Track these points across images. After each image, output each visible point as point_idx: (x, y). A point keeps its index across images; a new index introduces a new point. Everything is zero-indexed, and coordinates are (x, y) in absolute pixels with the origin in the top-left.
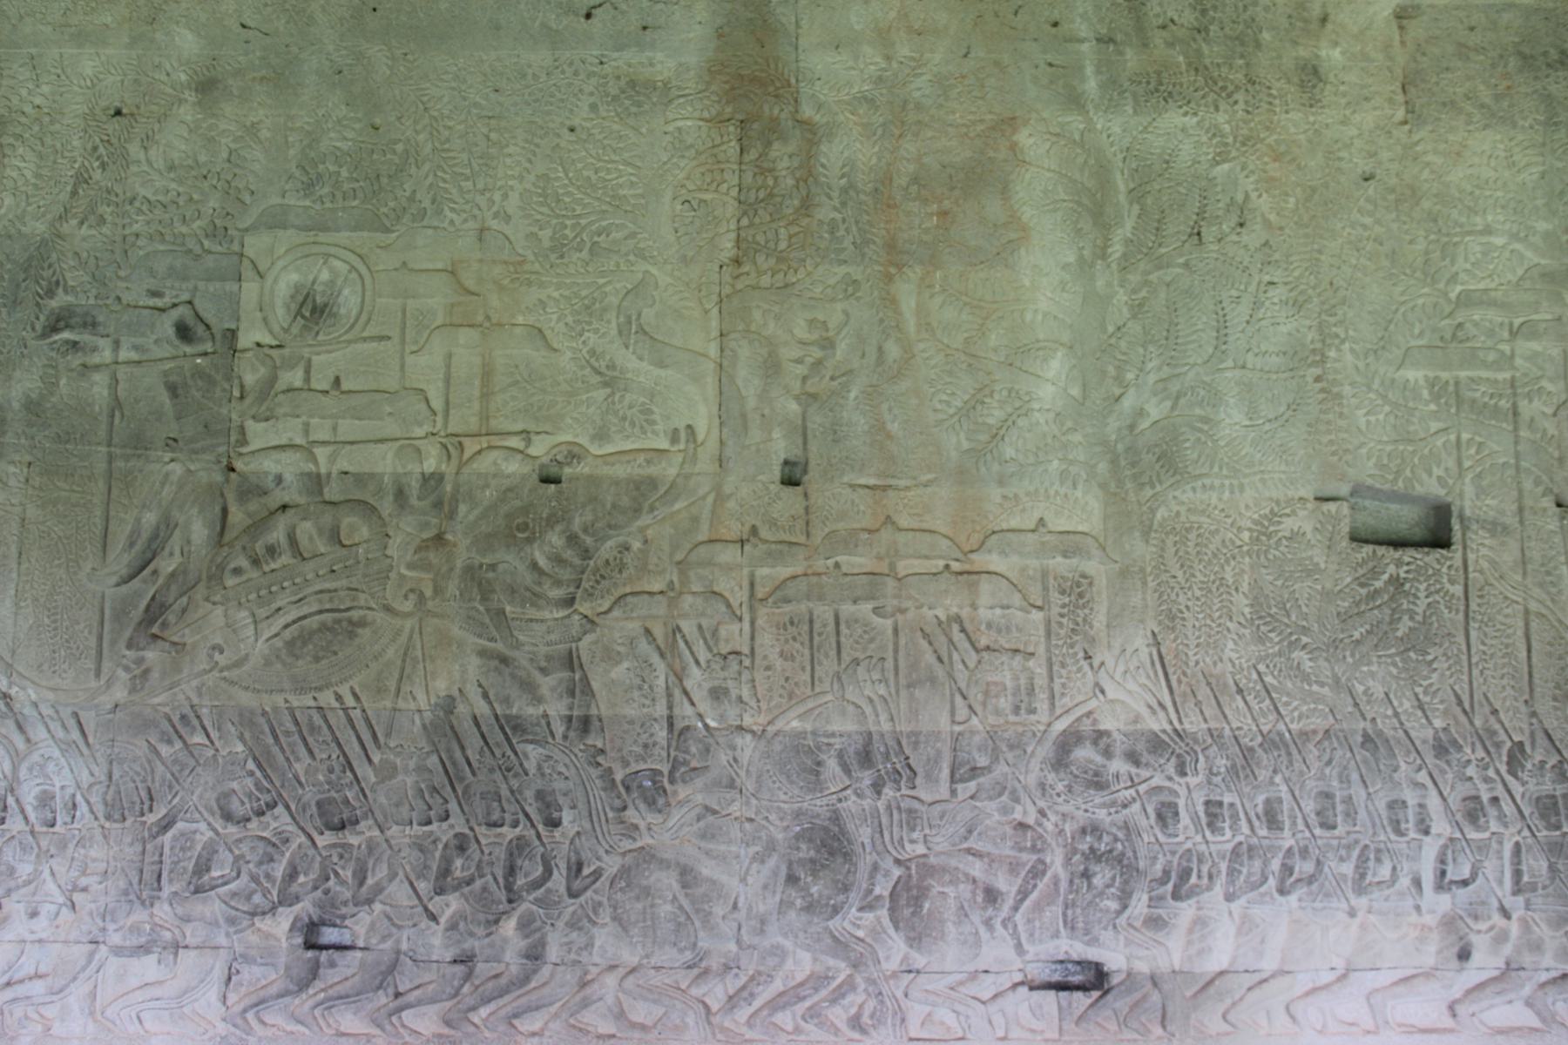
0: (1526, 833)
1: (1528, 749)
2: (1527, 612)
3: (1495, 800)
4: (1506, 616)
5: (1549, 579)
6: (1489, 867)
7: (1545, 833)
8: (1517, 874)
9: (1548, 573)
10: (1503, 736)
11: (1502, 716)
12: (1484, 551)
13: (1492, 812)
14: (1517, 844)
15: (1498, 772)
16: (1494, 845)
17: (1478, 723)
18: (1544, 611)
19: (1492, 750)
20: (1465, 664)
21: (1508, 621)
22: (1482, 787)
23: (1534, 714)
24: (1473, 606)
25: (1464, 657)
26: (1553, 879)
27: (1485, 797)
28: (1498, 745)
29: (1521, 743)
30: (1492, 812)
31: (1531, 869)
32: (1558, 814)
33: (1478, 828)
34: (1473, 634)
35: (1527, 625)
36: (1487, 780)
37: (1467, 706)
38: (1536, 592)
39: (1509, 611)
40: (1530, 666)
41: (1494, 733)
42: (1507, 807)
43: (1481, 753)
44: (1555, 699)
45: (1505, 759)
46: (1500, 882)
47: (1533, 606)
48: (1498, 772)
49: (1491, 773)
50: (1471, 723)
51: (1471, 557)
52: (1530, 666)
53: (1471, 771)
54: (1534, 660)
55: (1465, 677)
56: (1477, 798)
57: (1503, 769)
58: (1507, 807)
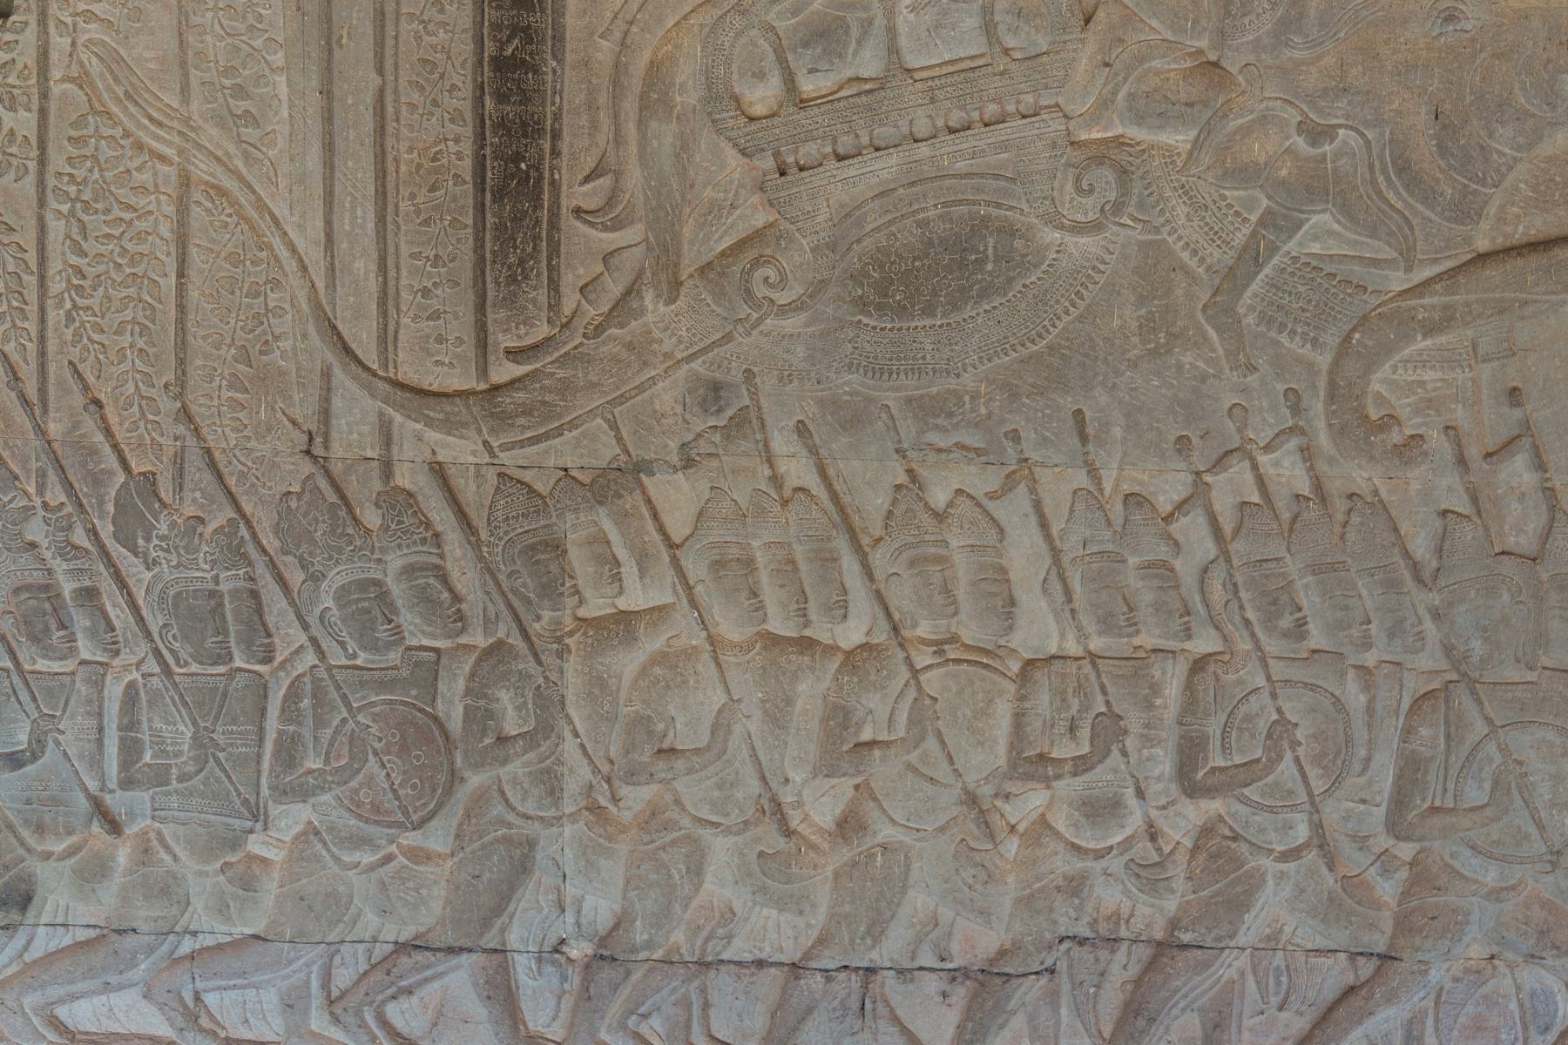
0: (152, 666)
1: (166, 491)
2: (185, 181)
3: (89, 595)
4: (142, 189)
5: (241, 106)
6: (72, 731)
7: (195, 668)
8: (131, 750)
9: (240, 92)
10: (112, 461)
11: (109, 411)
12: (93, 31)
13: (81, 621)
14: (131, 696)
15: (93, 532)
16: (82, 688)
17: (54, 429)
18: (228, 183)
19: (82, 488)
20: (32, 296)
21: (141, 202)
22: (60, 566)
23: (186, 415)
24: (57, 162)
25: (31, 280)
26: (201, 763)
27: (67, 588)
28: (98, 480)
29: (150, 479)
30: (81, 621)
31: (158, 739)
32: (222, 631)
33: (48, 652)
34: (56, 228)
35: (183, 209)
36: (68, 550)
37: (32, 392)
38: (211, 134)
39: (146, 177)
40: (181, 308)
41: (94, 452)
42: (118, 613)
43: (56, 495)
44: (235, 383)
45: (111, 508)
46: (96, 763)
47: (202, 168)
48: (93, 532)
49: (80, 537)
50: (41, 431)
51: (60, 43)
52: (181, 308)
53: (36, 531)
54: (194, 294)
55: (32, 326)
56: (48, 590)
57: (106, 531)
58: (118, 613)
